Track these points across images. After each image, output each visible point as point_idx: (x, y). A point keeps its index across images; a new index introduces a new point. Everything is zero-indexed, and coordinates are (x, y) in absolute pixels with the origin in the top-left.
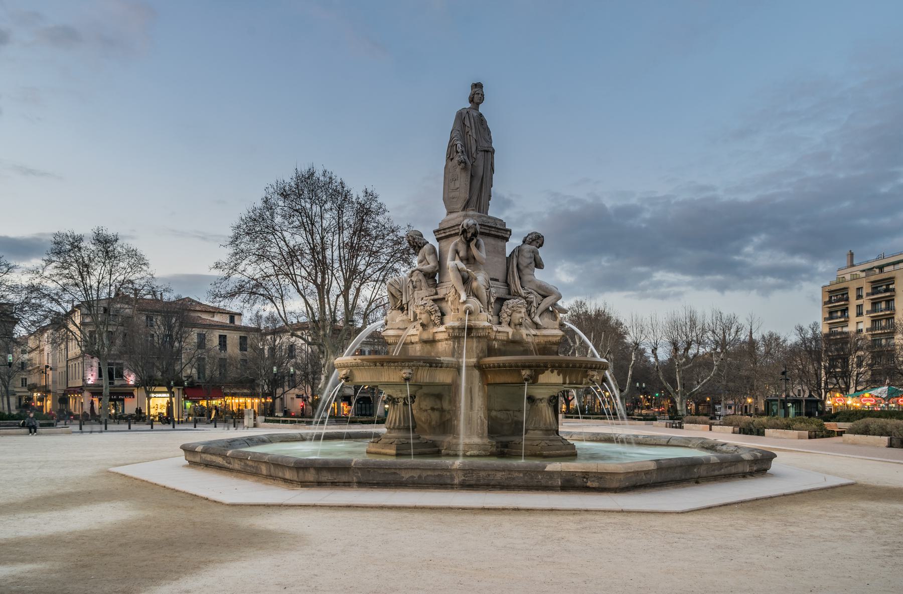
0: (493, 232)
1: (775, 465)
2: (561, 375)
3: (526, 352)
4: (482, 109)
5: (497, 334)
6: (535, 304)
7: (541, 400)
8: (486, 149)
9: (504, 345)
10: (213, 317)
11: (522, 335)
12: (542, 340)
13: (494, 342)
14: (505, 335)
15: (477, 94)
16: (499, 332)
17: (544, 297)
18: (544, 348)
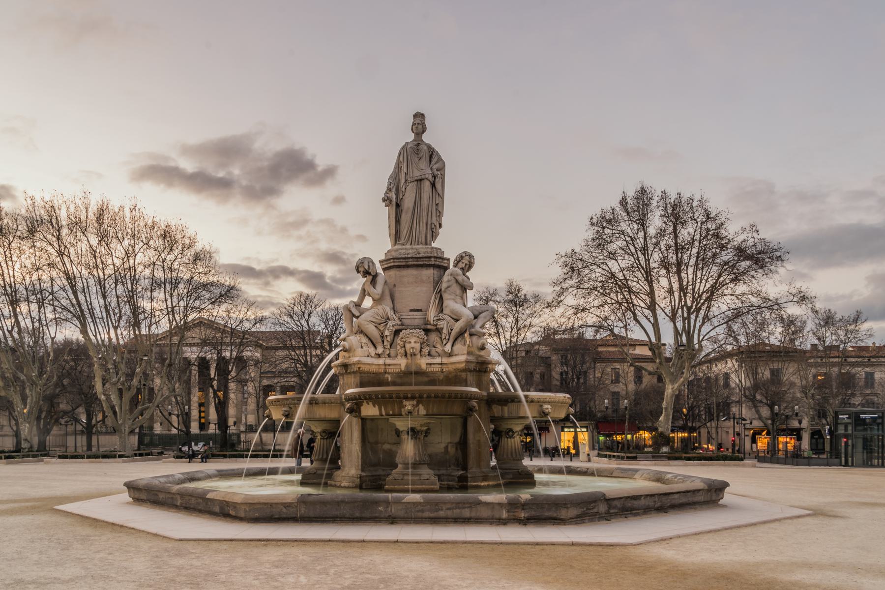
0: (411, 263)
1: (727, 497)
2: (377, 406)
3: (433, 382)
4: (426, 138)
5: (387, 367)
6: (445, 331)
7: (402, 432)
8: (419, 178)
9: (401, 377)
10: (635, 350)
11: (420, 366)
12: (451, 368)
13: (387, 375)
14: (398, 367)
15: (419, 123)
16: (389, 365)
17: (457, 320)
18: (456, 376)
